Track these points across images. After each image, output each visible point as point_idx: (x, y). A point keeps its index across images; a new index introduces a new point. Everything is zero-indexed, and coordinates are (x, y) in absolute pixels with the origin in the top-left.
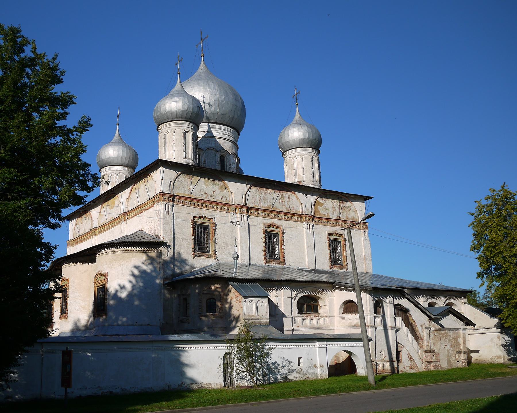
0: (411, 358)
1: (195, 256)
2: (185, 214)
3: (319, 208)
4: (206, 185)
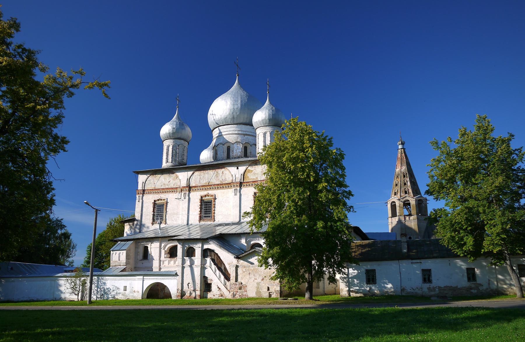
1: (153, 224)
4: (165, 179)
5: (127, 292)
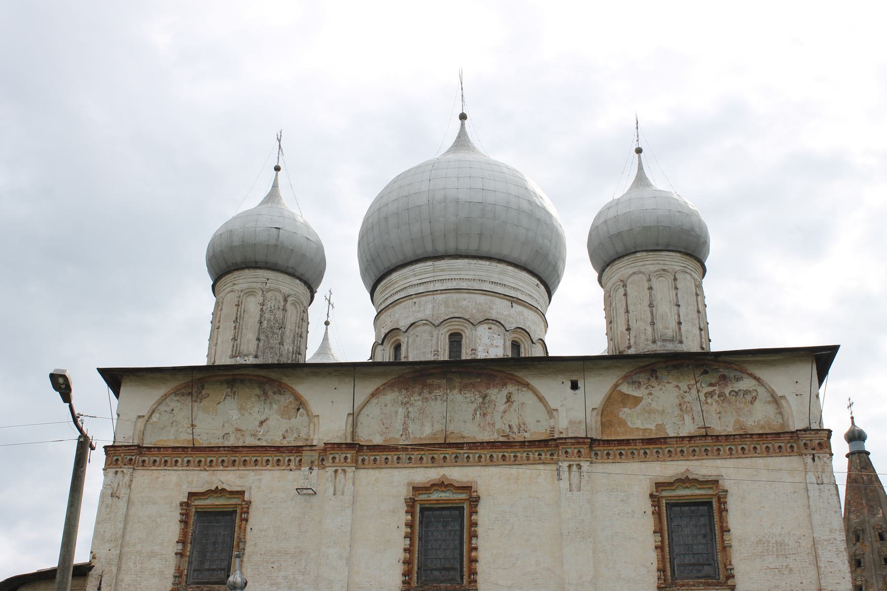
4: (242, 409)
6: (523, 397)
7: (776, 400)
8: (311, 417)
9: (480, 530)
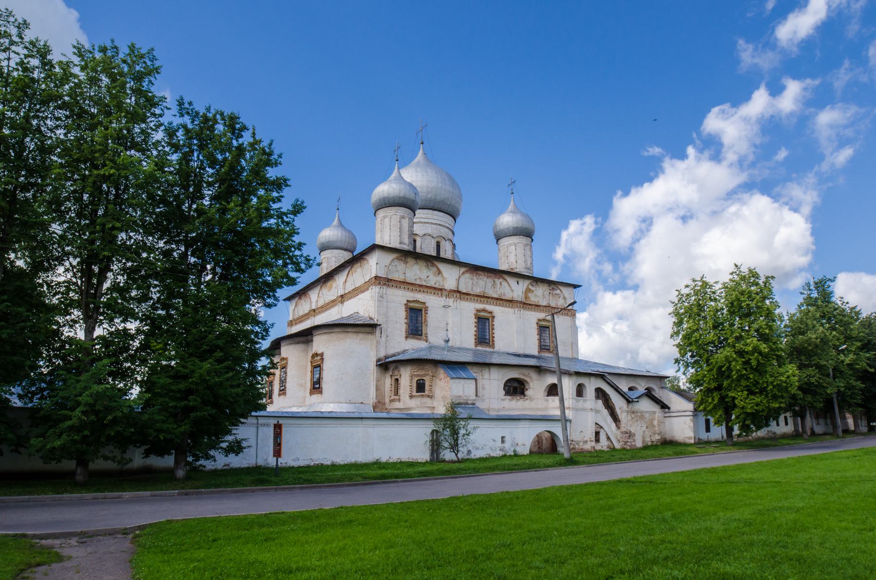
0: (608, 438)
2: (400, 297)
3: (530, 295)
5: (507, 445)
6: (504, 284)
7: (565, 298)
8: (444, 279)
9: (495, 327)
